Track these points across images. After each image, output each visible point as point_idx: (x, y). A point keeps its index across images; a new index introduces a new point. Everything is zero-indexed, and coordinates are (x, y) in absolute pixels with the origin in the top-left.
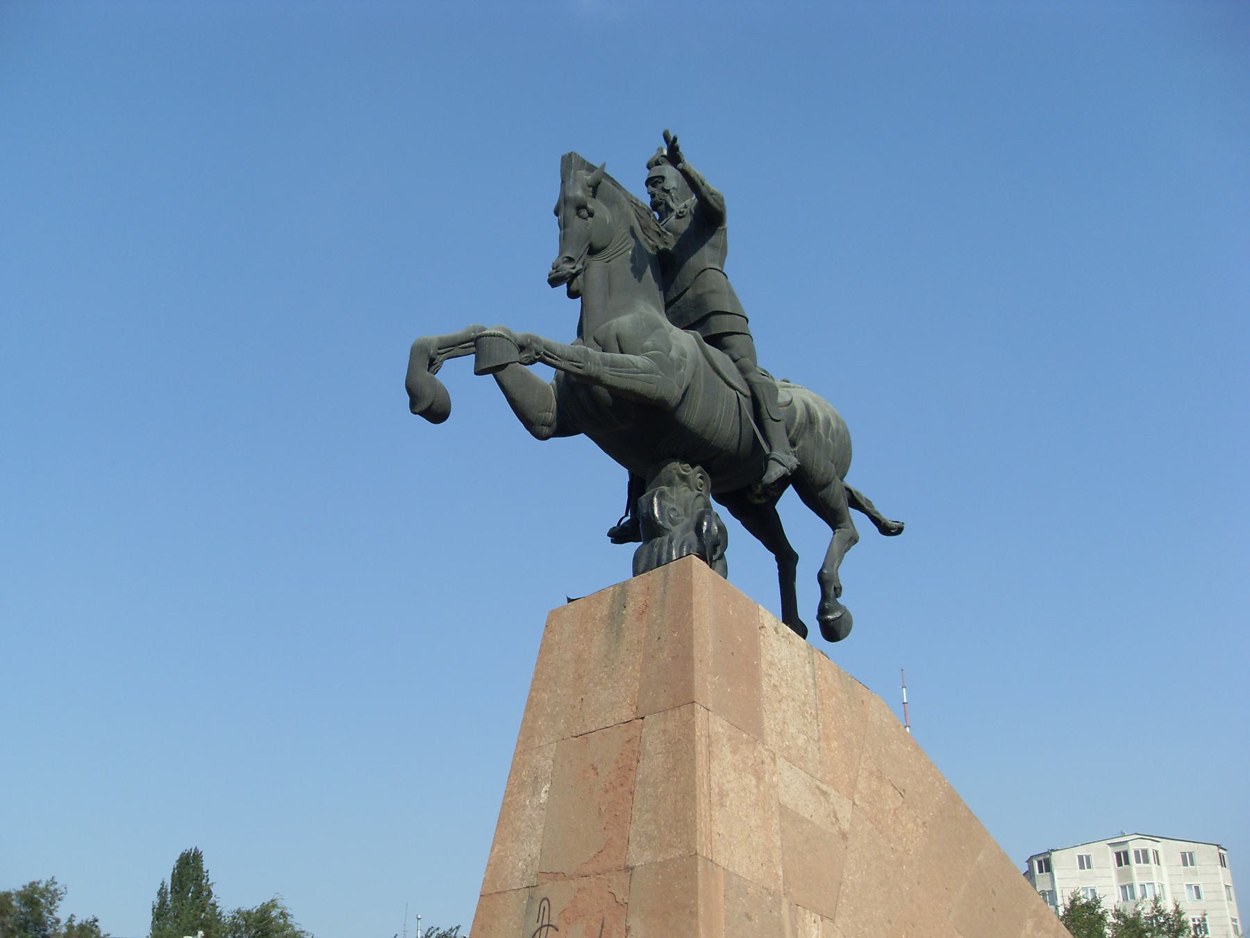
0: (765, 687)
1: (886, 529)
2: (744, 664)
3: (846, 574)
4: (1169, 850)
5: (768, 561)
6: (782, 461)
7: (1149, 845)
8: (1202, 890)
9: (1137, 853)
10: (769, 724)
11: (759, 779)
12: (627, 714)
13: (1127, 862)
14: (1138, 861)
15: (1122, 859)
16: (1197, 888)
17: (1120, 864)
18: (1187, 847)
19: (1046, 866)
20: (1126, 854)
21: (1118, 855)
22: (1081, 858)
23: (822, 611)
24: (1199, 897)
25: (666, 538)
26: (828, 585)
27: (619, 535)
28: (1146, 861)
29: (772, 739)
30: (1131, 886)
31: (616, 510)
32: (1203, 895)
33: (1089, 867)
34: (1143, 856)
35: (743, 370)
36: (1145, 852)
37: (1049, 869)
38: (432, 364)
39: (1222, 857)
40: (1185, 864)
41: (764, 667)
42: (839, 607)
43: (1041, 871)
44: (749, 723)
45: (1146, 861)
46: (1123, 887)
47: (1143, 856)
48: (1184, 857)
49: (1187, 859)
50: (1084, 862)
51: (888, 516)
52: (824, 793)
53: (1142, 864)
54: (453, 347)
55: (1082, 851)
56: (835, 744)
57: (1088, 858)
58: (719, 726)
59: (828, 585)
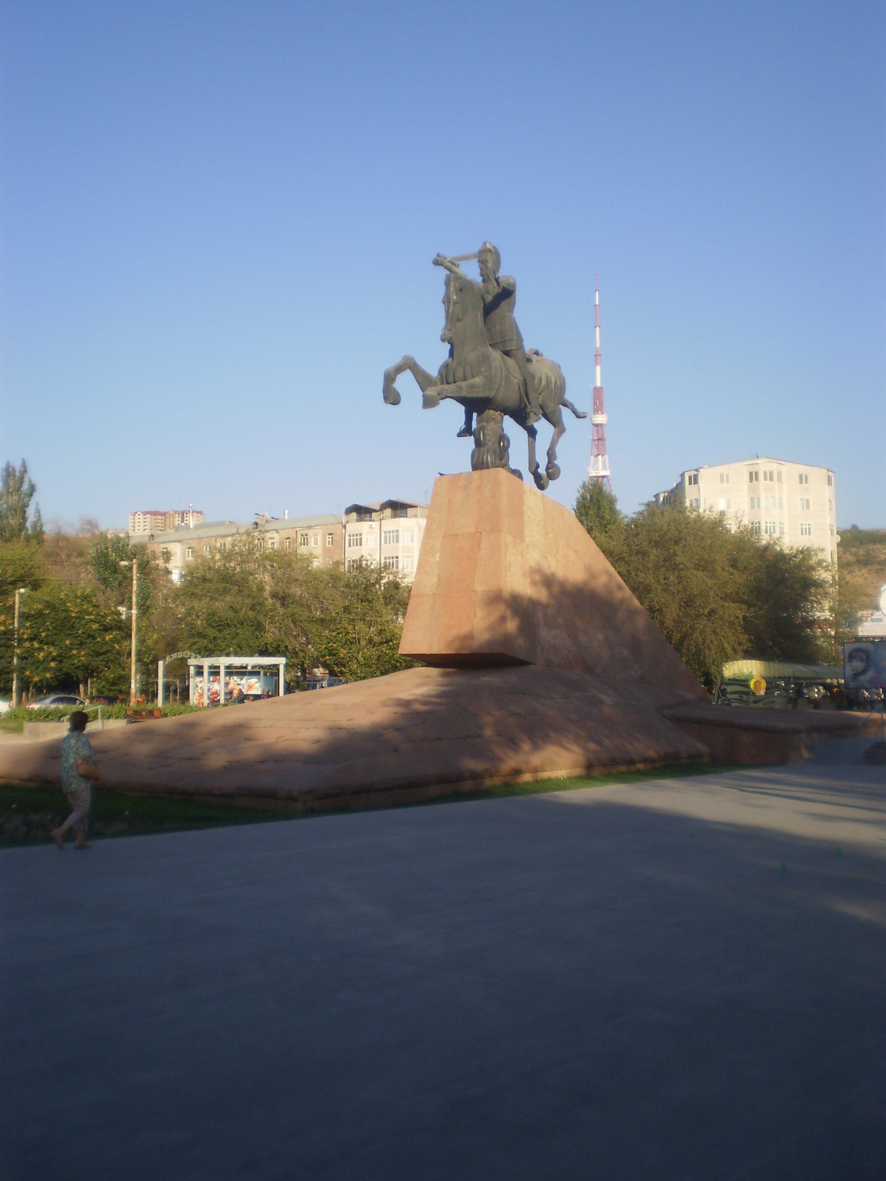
0: (525, 518)
1: (578, 417)
2: (518, 512)
3: (558, 450)
4: (790, 471)
5: (524, 433)
6: (536, 399)
7: (774, 467)
8: (811, 502)
9: (765, 473)
10: (527, 533)
11: (522, 556)
12: (472, 530)
13: (757, 479)
14: (765, 479)
15: (753, 477)
16: (808, 501)
17: (751, 480)
18: (803, 469)
19: (694, 480)
20: (756, 474)
21: (751, 474)
22: (722, 475)
23: (547, 469)
24: (808, 507)
25: (486, 448)
26: (551, 455)
27: (459, 435)
28: (771, 479)
29: (527, 540)
30: (759, 499)
31: (461, 423)
32: (811, 507)
33: (727, 482)
34: (769, 476)
35: (520, 367)
36: (771, 473)
37: (696, 482)
38: (393, 380)
39: (829, 478)
40: (801, 482)
41: (525, 508)
42: (555, 466)
43: (690, 484)
44: (519, 536)
45: (771, 479)
46: (752, 499)
47: (769, 476)
48: (801, 476)
49: (802, 479)
50: (723, 479)
51: (580, 409)
52: (546, 557)
53: (768, 481)
54: (399, 369)
55: (723, 469)
56: (551, 535)
57: (727, 476)
58: (509, 538)
59: (551, 455)
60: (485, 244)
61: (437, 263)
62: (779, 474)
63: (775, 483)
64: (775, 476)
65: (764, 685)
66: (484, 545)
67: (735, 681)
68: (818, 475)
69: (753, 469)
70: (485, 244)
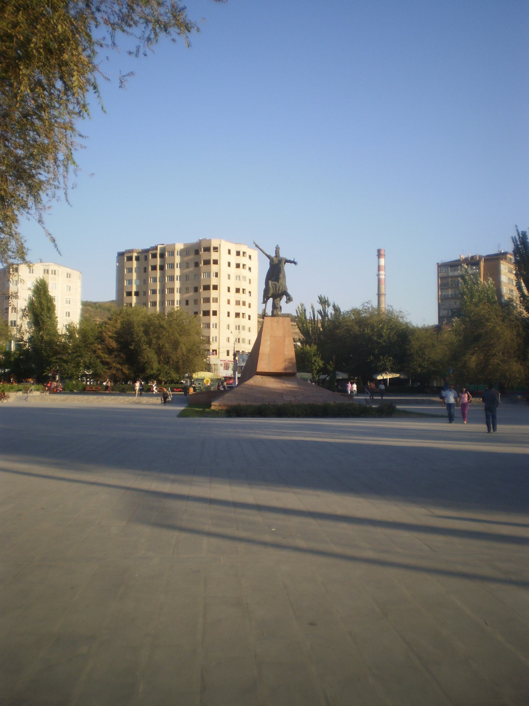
8: (71, 288)
9: (52, 271)
16: (70, 287)
18: (69, 271)
20: (48, 271)
21: (45, 270)
24: (70, 290)
36: (55, 271)
48: (68, 274)
49: (69, 276)
53: (53, 275)
60: (277, 245)
61: (257, 246)
62: (58, 271)
63: (56, 276)
64: (57, 272)
65: (210, 382)
66: (286, 340)
67: (197, 380)
68: (76, 275)
69: (46, 268)
70: (277, 245)
